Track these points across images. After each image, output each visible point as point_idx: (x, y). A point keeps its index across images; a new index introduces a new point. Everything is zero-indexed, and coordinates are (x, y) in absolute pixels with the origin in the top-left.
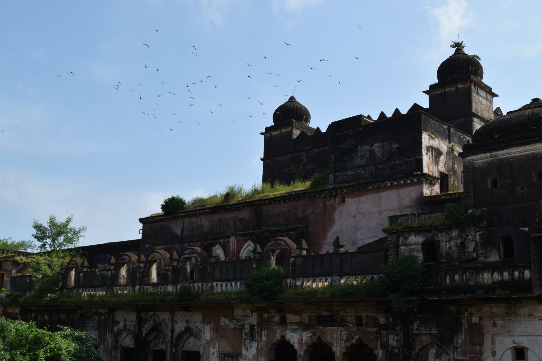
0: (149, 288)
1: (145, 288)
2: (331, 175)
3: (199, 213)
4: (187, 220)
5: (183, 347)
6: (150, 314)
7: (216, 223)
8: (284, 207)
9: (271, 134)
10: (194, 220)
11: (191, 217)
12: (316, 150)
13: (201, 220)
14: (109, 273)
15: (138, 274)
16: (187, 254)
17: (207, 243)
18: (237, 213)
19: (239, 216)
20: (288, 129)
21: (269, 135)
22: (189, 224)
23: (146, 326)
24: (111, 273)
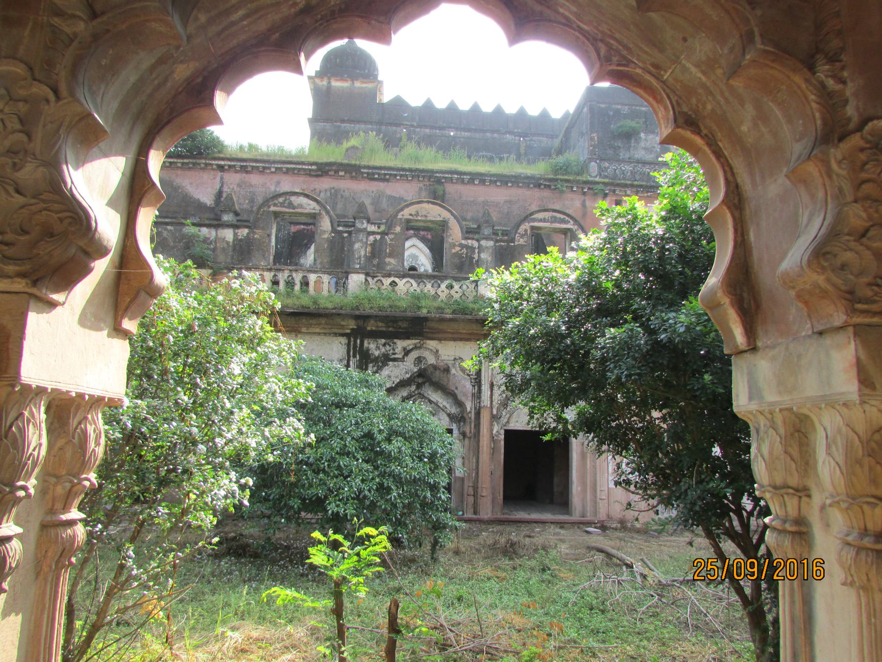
0: (402, 283)
1: (387, 281)
2: (593, 163)
3: (277, 169)
4: (233, 179)
5: (508, 422)
6: (400, 344)
7: (322, 195)
8: (499, 195)
9: (329, 83)
10: (255, 179)
11: (247, 172)
12: (427, 131)
13: (278, 183)
14: (228, 234)
15: (357, 246)
16: (540, 221)
17: (293, 229)
18: (382, 185)
19: (389, 192)
20: (370, 86)
21: (325, 83)
22: (239, 186)
23: (386, 371)
24: (235, 235)
